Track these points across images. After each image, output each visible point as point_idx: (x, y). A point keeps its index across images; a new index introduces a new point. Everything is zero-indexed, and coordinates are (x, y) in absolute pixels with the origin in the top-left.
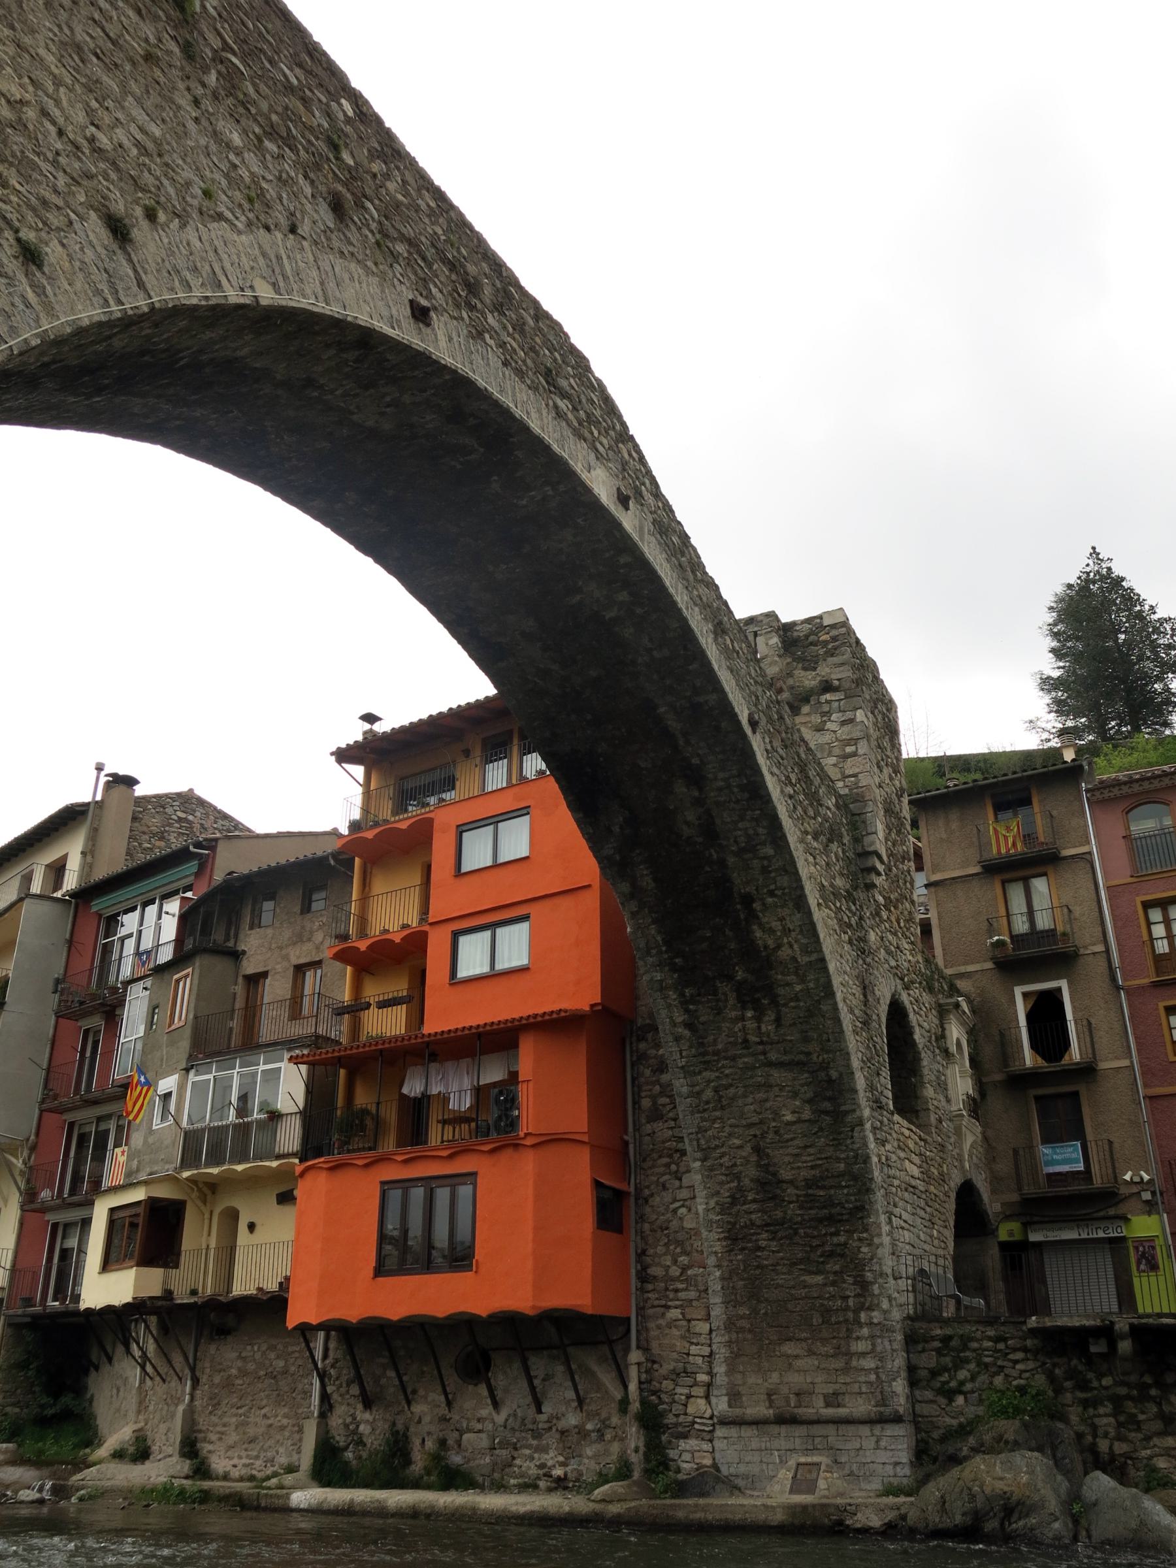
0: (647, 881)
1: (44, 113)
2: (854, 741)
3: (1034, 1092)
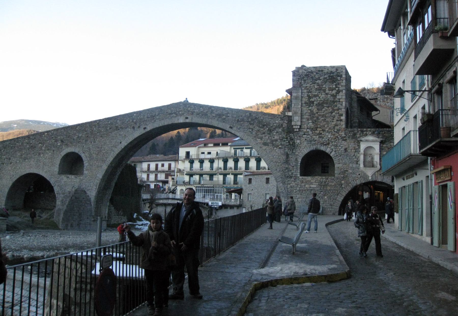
1: (108, 148)
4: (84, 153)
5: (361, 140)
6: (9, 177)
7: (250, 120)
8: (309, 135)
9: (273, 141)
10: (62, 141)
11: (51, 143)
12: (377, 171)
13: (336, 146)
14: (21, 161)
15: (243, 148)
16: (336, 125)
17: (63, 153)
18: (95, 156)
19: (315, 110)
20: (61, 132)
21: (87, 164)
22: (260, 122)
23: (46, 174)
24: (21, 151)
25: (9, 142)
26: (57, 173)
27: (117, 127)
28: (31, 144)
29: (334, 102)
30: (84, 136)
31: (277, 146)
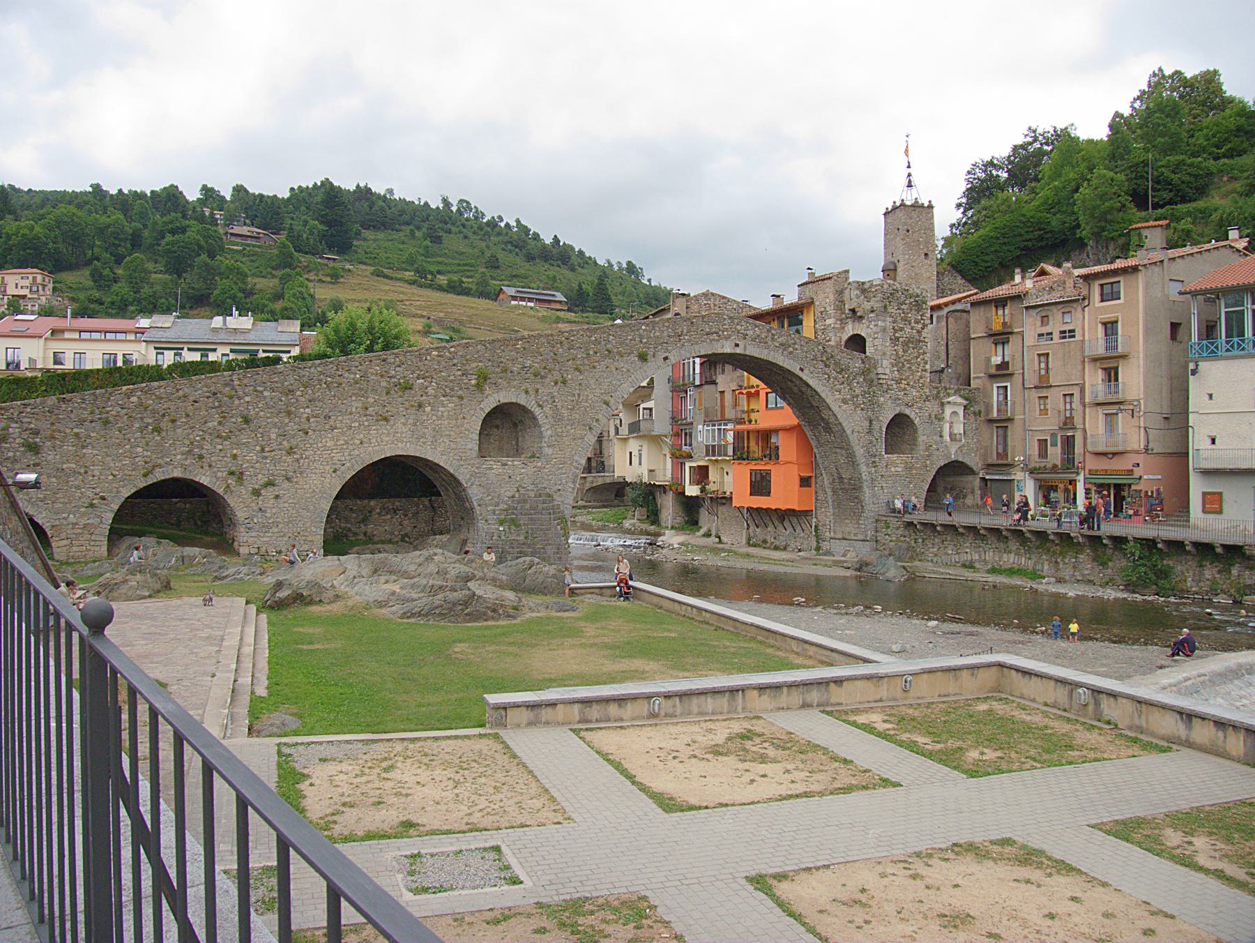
2: (877, 333)
4: (539, 406)
5: (949, 402)
6: (328, 468)
11: (452, 378)
13: (920, 408)
14: (366, 423)
15: (182, 349)
16: (921, 377)
17: (489, 404)
18: (565, 413)
19: (900, 349)
23: (444, 457)
24: (363, 396)
25: (319, 369)
26: (475, 453)
29: (920, 341)
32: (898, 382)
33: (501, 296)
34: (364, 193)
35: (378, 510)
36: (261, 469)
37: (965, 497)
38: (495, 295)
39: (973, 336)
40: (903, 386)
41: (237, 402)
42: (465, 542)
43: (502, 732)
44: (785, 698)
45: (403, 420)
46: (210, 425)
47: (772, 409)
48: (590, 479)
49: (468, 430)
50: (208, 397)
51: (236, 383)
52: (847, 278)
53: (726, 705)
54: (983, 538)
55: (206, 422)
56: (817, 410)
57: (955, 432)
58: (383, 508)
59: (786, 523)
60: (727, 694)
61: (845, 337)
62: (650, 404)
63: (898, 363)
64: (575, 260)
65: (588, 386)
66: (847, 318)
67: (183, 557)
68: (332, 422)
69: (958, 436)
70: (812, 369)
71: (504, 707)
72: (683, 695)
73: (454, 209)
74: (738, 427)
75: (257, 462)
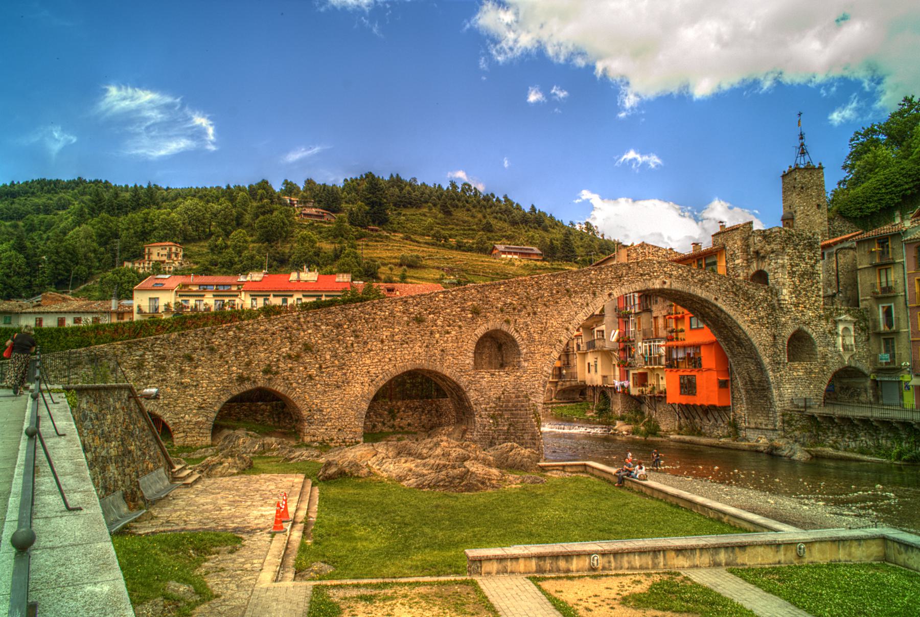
0: (709, 323)
2: (778, 268)
3: (882, 337)
4: (517, 331)
5: (841, 320)
6: (366, 379)
7: (734, 290)
8: (792, 311)
9: (759, 318)
10: (476, 312)
11: (454, 313)
12: (852, 356)
13: (816, 326)
15: (269, 296)
17: (480, 331)
18: (536, 336)
20: (472, 294)
21: (525, 351)
22: (745, 293)
23: (449, 370)
24: (391, 327)
27: (568, 291)
28: (412, 313)
29: (813, 273)
30: (514, 302)
31: (762, 325)
32: (796, 305)
33: (495, 252)
34: (396, 181)
35: (403, 409)
36: (319, 381)
37: (859, 395)
38: (490, 251)
39: (860, 267)
40: (800, 309)
41: (302, 334)
42: (465, 432)
43: (477, 578)
44: (698, 559)
45: (419, 344)
46: (284, 350)
47: (695, 329)
48: (560, 383)
49: (466, 350)
50: (282, 331)
51: (302, 320)
52: (751, 228)
53: (650, 563)
54: (876, 429)
55: (280, 348)
56: (731, 330)
57: (848, 343)
58: (407, 407)
59: (710, 416)
60: (651, 554)
61: (751, 272)
62: (603, 327)
63: (795, 291)
64: (547, 222)
65: (552, 316)
66: (752, 258)
67: (263, 444)
68: (369, 347)
69: (850, 347)
70: (724, 298)
71: (480, 560)
72: (616, 554)
73: (459, 190)
74: (670, 343)
75: (317, 375)
